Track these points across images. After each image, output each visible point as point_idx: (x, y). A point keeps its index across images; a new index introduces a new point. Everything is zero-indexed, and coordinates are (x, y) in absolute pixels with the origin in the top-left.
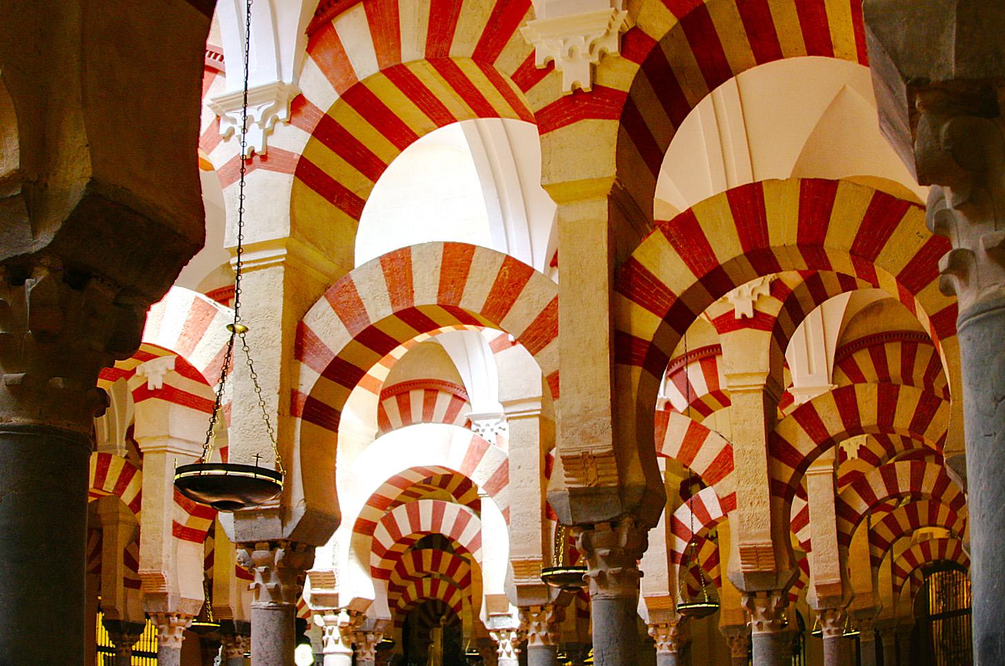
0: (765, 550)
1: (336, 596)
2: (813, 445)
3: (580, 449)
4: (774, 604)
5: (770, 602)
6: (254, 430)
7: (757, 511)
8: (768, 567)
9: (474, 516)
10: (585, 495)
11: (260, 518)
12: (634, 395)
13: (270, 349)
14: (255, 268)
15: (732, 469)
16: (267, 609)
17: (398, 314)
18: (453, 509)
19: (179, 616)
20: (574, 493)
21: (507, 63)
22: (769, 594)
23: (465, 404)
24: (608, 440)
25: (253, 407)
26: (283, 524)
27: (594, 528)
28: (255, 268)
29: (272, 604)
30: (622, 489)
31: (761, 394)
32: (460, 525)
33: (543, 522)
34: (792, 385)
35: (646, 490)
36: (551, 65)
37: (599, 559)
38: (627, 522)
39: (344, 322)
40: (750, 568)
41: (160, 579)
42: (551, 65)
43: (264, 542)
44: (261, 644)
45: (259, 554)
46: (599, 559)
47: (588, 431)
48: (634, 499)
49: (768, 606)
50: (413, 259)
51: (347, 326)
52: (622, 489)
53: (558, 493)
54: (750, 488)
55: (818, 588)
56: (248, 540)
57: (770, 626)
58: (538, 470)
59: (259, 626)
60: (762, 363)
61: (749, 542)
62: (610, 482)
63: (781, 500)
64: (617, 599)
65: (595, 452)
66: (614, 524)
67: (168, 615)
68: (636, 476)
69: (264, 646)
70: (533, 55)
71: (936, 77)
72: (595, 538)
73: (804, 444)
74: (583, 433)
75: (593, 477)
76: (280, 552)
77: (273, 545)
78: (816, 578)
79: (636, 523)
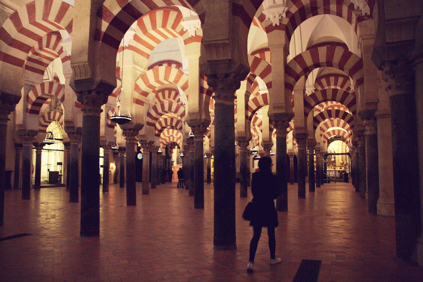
1: (146, 140)
2: (256, 107)
12: (204, 100)
21: (179, 29)
22: (244, 142)
27: (195, 127)
35: (205, 120)
36: (187, 31)
42: (187, 31)
45: (128, 131)
63: (248, 120)
65: (195, 112)
67: (106, 146)
68: (203, 117)
70: (183, 29)
75: (195, 117)
76: (131, 131)
77: (130, 130)
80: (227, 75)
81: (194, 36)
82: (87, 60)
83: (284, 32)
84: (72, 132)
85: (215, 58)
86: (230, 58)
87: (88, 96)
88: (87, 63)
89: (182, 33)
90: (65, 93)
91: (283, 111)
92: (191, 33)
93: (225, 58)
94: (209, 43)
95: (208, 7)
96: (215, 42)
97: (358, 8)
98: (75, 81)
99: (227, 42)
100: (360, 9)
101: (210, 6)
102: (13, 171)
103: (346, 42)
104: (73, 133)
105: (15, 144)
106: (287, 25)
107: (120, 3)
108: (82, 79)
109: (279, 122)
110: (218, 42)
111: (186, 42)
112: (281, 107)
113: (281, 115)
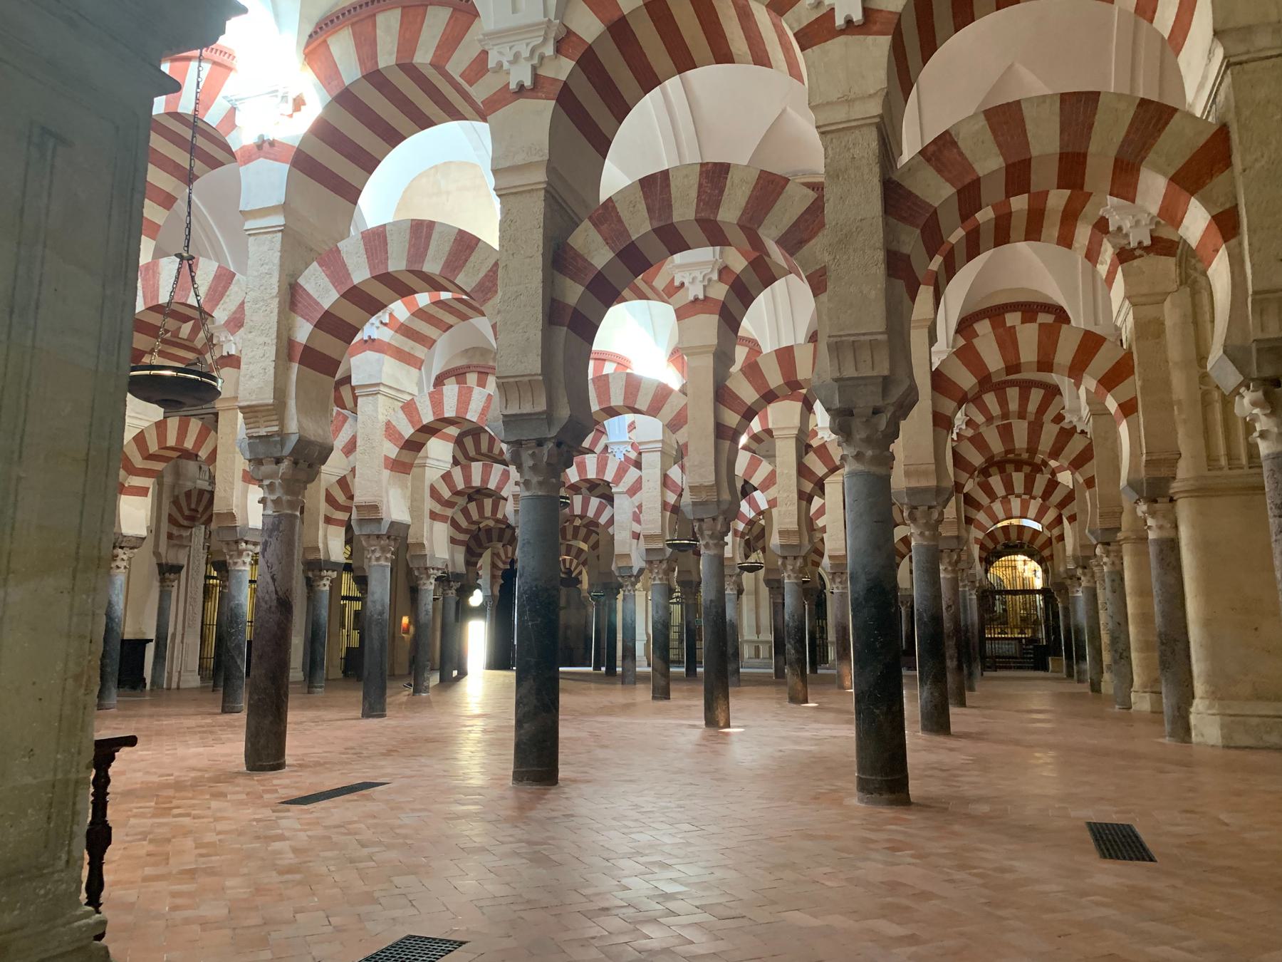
0: (794, 532)
2: (826, 470)
4: (798, 564)
5: (796, 564)
7: (790, 508)
8: (795, 541)
9: (609, 507)
15: (774, 484)
17: (601, 409)
18: (595, 502)
19: (433, 569)
20: (694, 504)
22: (795, 558)
23: (604, 436)
24: (714, 479)
30: (719, 502)
31: (794, 440)
32: (599, 512)
33: (662, 512)
34: (817, 425)
38: (721, 519)
40: (785, 542)
41: (422, 545)
48: (724, 507)
49: (794, 566)
50: (610, 380)
52: (719, 502)
54: (785, 495)
55: (830, 557)
57: (796, 578)
58: (659, 483)
60: (796, 421)
61: (784, 527)
64: (715, 555)
65: (706, 484)
66: (714, 519)
67: (426, 569)
71: (834, 407)
72: (704, 526)
73: (819, 469)
75: (704, 497)
78: (829, 550)
79: (725, 519)
80: (876, 411)
81: (701, 297)
82: (539, 372)
83: (932, 288)
84: (376, 533)
85: (850, 372)
86: (886, 373)
87: (536, 451)
88: (541, 378)
89: (670, 292)
90: (359, 435)
91: (932, 482)
92: (695, 291)
93: (875, 373)
94: (839, 339)
95: (834, 259)
96: (852, 338)
97: (1120, 229)
98: (505, 416)
99: (880, 337)
100: (1124, 232)
101: (838, 257)
102: (151, 640)
103: (1063, 302)
104: (378, 536)
105: (160, 565)
106: (937, 273)
107: (610, 241)
108: (525, 412)
109: (921, 508)
110: (862, 338)
111: (681, 314)
112: (925, 474)
113: (925, 490)
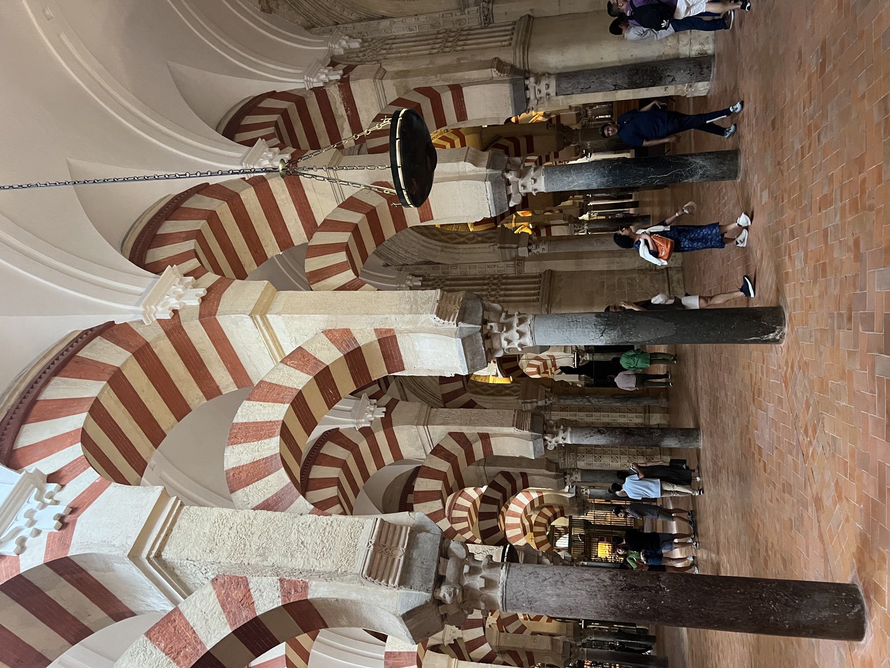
3: (434, 304)
6: (325, 541)
10: (464, 314)
11: (415, 554)
13: (255, 522)
14: (167, 535)
16: (508, 571)
25: (302, 543)
26: (428, 532)
28: (167, 535)
29: (504, 567)
37: (508, 320)
39: (265, 476)
43: (439, 562)
44: (545, 580)
45: (450, 570)
46: (508, 320)
47: (423, 301)
51: (270, 474)
53: (458, 332)
56: (433, 576)
59: (526, 581)
62: (460, 299)
69: (547, 576)
74: (424, 304)
